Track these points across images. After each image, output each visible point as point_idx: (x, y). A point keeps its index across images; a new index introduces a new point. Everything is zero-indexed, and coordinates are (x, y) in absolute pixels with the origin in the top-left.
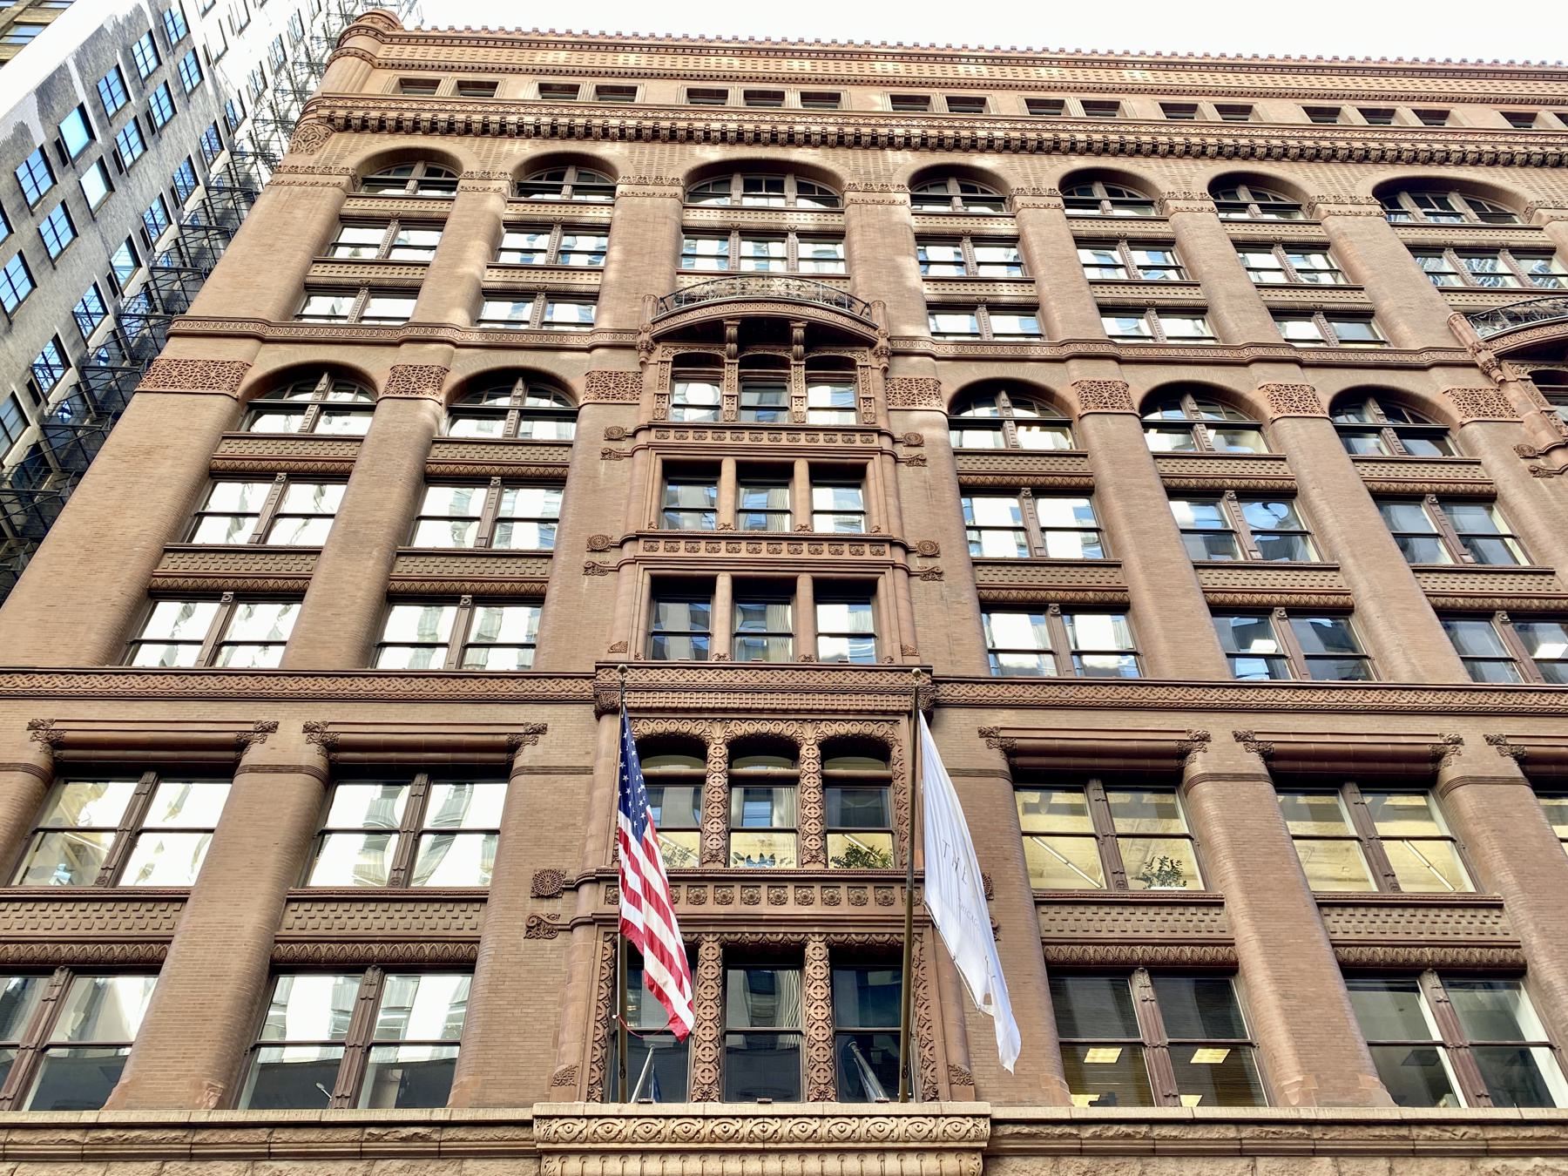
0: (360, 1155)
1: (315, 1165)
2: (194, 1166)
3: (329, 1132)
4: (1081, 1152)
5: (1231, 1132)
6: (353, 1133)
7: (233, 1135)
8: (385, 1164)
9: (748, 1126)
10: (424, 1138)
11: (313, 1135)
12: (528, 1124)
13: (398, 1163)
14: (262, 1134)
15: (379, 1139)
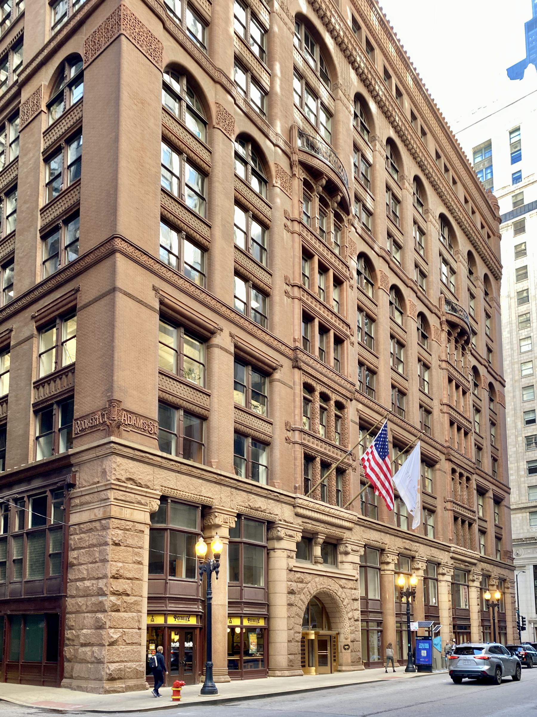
0: (265, 497)
1: (260, 498)
2: (237, 491)
3: (262, 490)
4: (363, 526)
5: (380, 527)
6: (266, 492)
7: (246, 486)
8: (270, 501)
9: (323, 508)
10: (277, 496)
11: (259, 490)
12: (294, 498)
13: (272, 501)
14: (250, 487)
15: (271, 495)
